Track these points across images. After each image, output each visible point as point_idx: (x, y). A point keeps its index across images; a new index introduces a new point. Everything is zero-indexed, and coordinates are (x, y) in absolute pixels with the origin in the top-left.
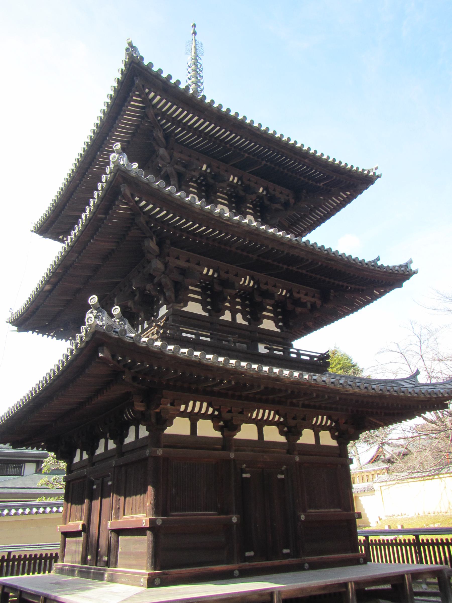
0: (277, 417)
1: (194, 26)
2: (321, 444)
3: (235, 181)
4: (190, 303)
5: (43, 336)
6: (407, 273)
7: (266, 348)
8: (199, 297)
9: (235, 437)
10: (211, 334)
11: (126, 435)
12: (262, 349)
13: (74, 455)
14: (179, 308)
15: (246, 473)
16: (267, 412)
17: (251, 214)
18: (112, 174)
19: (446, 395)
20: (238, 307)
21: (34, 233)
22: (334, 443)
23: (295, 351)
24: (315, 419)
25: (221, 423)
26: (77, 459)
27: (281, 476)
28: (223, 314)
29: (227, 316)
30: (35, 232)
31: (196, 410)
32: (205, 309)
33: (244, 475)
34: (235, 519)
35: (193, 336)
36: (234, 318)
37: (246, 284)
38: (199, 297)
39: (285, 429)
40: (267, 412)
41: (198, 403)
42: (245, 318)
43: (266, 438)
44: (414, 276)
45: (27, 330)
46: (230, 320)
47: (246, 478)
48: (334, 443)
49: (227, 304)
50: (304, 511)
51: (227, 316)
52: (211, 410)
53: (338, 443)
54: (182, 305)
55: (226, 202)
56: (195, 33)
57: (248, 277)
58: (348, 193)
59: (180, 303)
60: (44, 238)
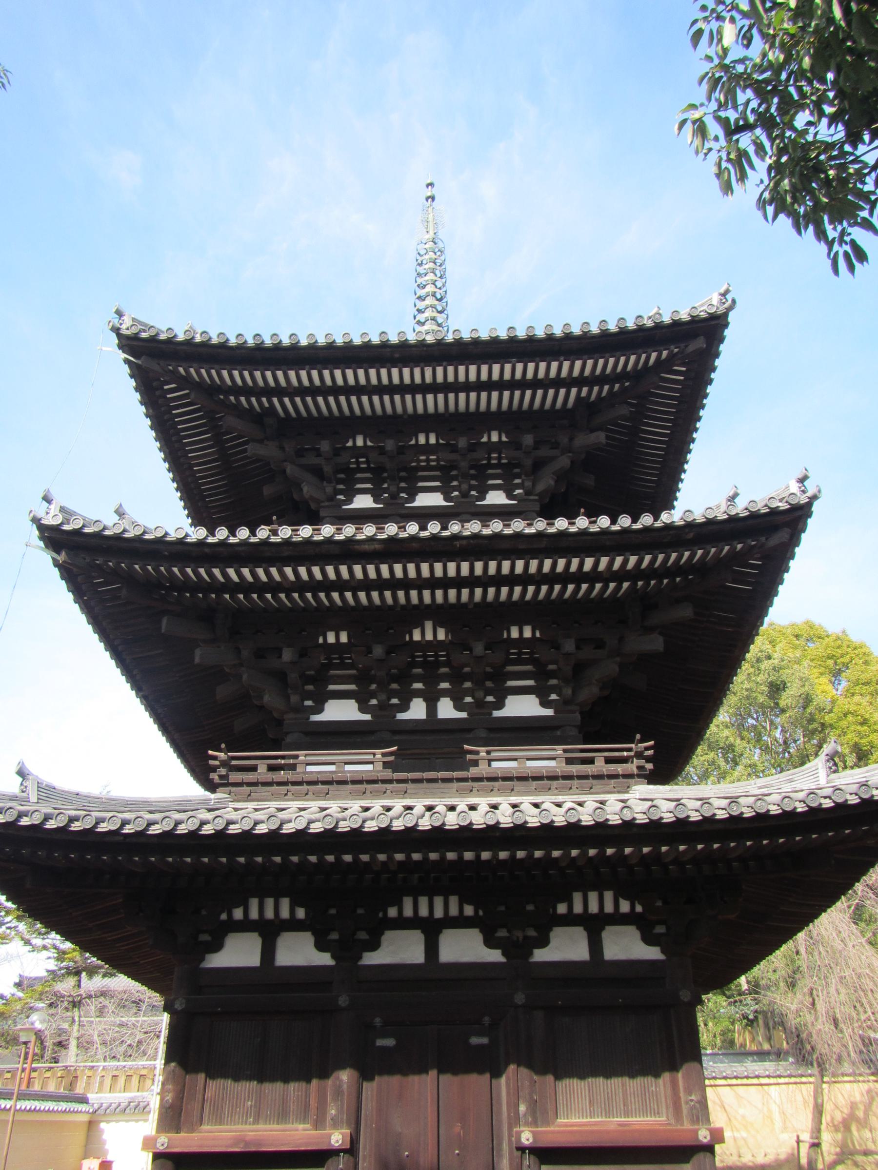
0: (469, 910)
15: (384, 1036)
27: (475, 1040)
28: (405, 707)
33: (380, 1042)
36: (432, 709)
42: (458, 707)
47: (384, 1048)
49: (418, 686)
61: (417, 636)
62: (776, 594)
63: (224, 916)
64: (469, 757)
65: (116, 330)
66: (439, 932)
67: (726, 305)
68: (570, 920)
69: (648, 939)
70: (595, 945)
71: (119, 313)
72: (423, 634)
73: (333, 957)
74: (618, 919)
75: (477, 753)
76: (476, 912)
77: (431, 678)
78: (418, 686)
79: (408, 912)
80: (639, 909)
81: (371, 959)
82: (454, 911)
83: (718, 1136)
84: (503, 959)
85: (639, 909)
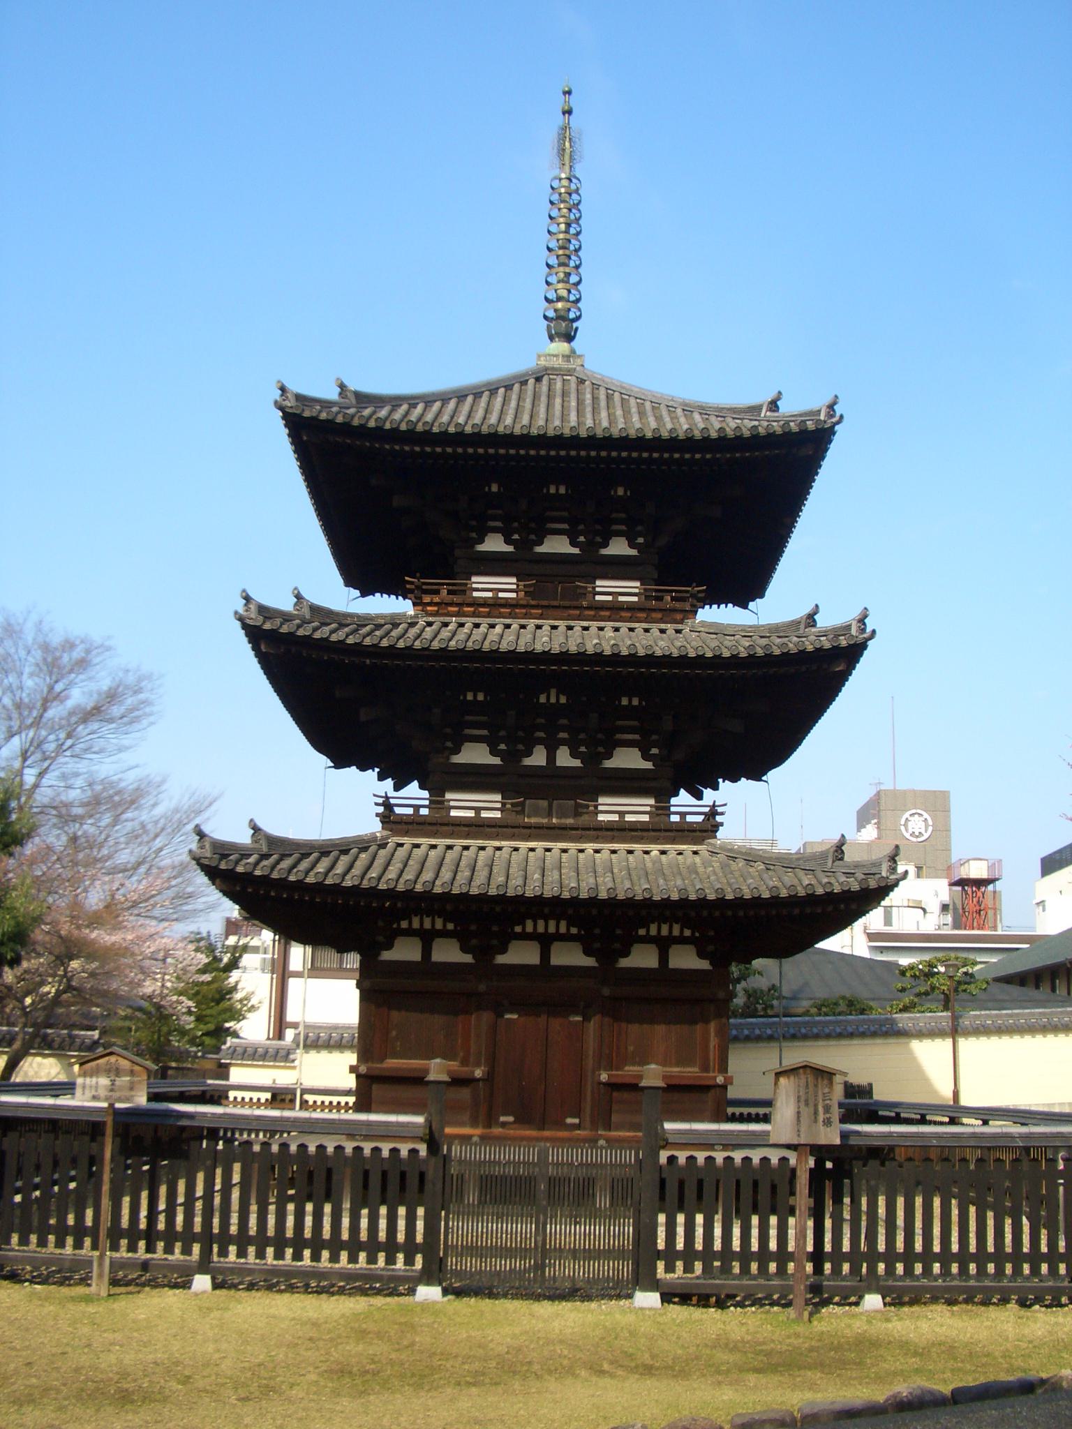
1: (569, 93)
14: (441, 760)
22: (704, 965)
28: (529, 754)
29: (538, 758)
32: (494, 752)
34: (478, 1073)
36: (551, 758)
37: (553, 700)
42: (574, 755)
44: (870, 643)
48: (704, 965)
49: (542, 734)
51: (538, 758)
56: (568, 112)
57: (553, 692)
61: (543, 699)
62: (847, 680)
63: (395, 926)
64: (579, 591)
65: (281, 408)
66: (552, 943)
67: (834, 420)
68: (647, 940)
69: (701, 955)
70: (664, 959)
71: (283, 389)
72: (548, 698)
74: (682, 940)
75: (588, 807)
76: (579, 931)
78: (542, 734)
79: (529, 928)
80: (697, 934)
81: (501, 959)
82: (563, 930)
83: (729, 1081)
84: (596, 965)
85: (697, 934)
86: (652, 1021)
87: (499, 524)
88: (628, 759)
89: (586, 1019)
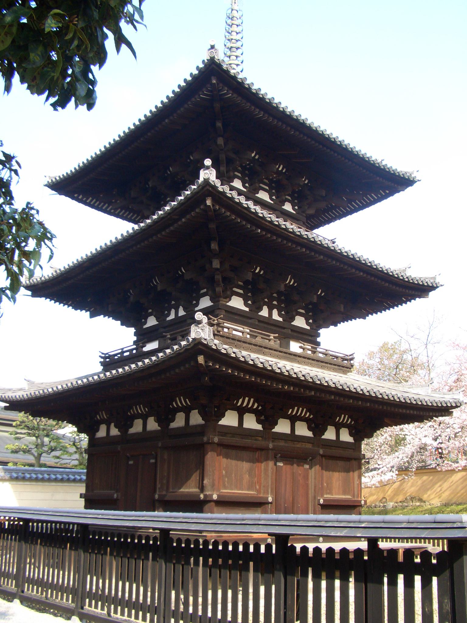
2: (341, 440)
3: (280, 169)
4: (234, 298)
5: (60, 304)
6: (435, 286)
7: (301, 347)
8: (241, 291)
9: (273, 430)
10: (250, 330)
11: (173, 420)
12: (295, 347)
13: (98, 430)
14: (225, 303)
16: (301, 409)
17: (289, 201)
18: (200, 187)
19: (454, 405)
20: (275, 303)
21: (47, 188)
22: (350, 439)
23: (324, 351)
24: (338, 418)
25: (263, 418)
26: (102, 433)
29: (264, 312)
30: (48, 187)
31: (245, 405)
32: (246, 304)
35: (240, 334)
36: (270, 314)
38: (241, 291)
39: (313, 425)
40: (301, 409)
41: (247, 399)
42: (280, 315)
43: (298, 432)
45: (40, 296)
46: (267, 316)
50: (322, 496)
52: (256, 406)
53: (354, 440)
54: (228, 299)
55: (267, 188)
57: (290, 276)
58: (387, 192)
59: (226, 298)
60: (58, 195)
73: (262, 427)
77: (271, 299)
86: (334, 470)
87: (240, 175)
88: (300, 322)
89: (311, 468)
